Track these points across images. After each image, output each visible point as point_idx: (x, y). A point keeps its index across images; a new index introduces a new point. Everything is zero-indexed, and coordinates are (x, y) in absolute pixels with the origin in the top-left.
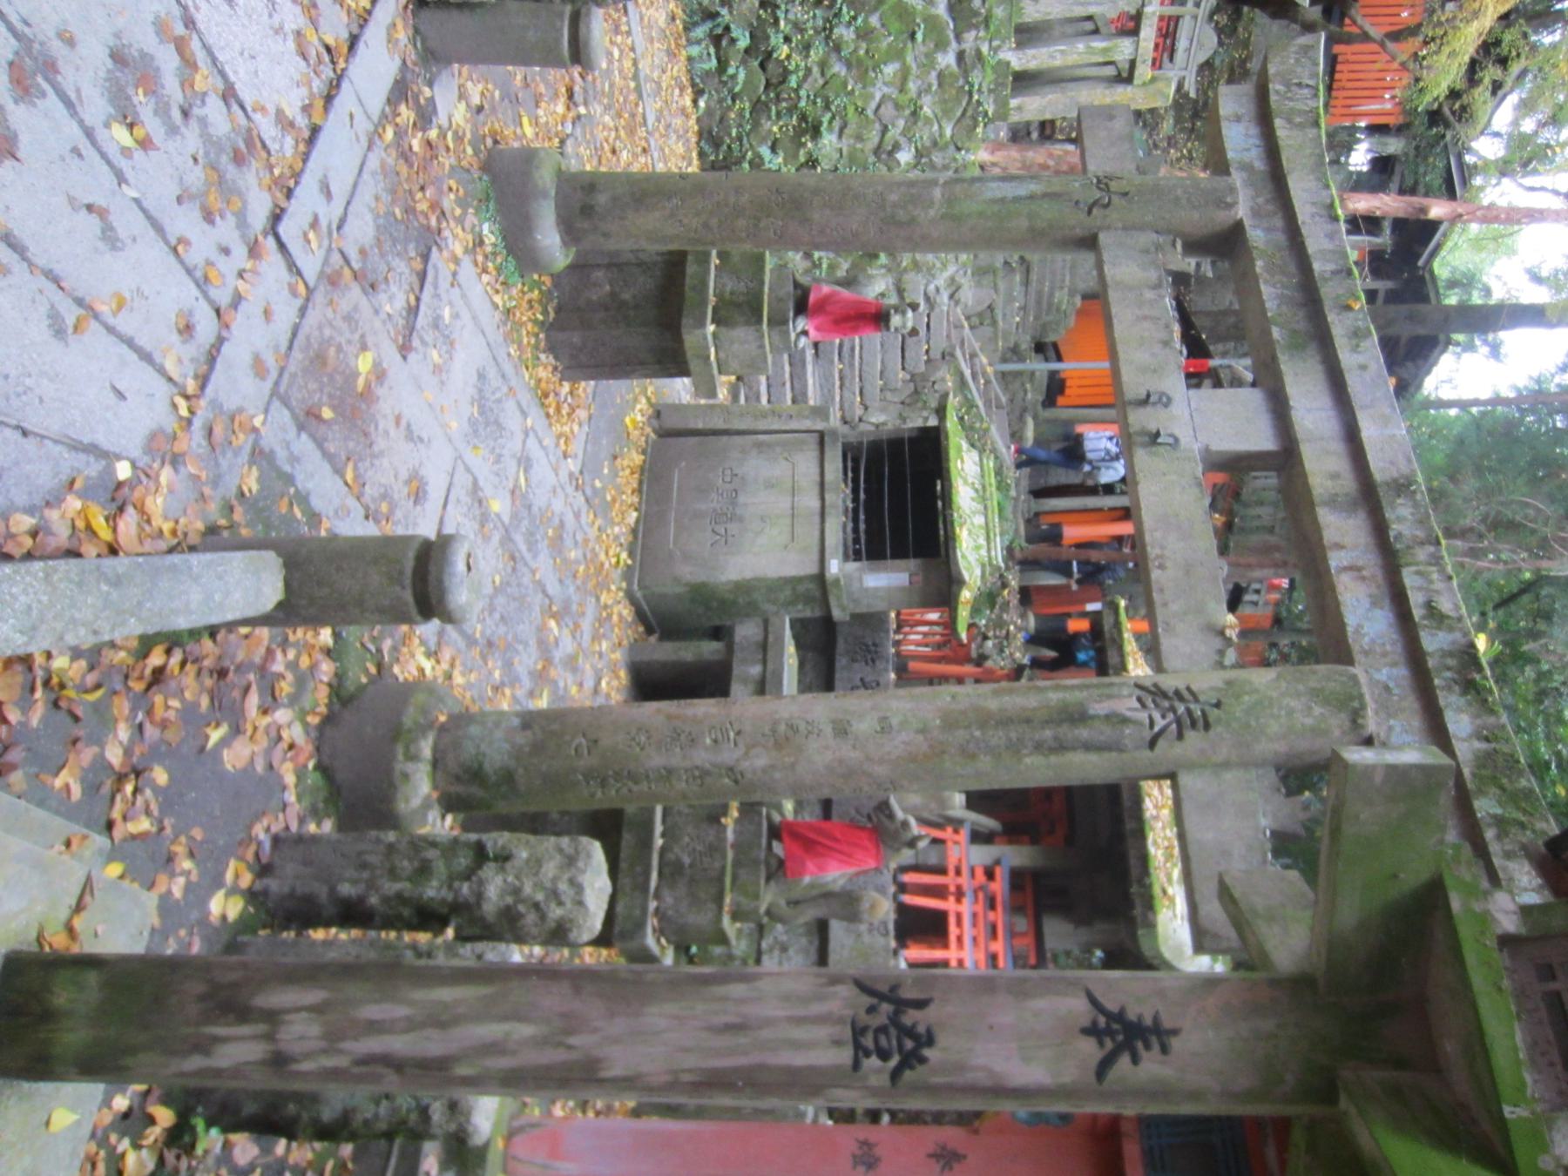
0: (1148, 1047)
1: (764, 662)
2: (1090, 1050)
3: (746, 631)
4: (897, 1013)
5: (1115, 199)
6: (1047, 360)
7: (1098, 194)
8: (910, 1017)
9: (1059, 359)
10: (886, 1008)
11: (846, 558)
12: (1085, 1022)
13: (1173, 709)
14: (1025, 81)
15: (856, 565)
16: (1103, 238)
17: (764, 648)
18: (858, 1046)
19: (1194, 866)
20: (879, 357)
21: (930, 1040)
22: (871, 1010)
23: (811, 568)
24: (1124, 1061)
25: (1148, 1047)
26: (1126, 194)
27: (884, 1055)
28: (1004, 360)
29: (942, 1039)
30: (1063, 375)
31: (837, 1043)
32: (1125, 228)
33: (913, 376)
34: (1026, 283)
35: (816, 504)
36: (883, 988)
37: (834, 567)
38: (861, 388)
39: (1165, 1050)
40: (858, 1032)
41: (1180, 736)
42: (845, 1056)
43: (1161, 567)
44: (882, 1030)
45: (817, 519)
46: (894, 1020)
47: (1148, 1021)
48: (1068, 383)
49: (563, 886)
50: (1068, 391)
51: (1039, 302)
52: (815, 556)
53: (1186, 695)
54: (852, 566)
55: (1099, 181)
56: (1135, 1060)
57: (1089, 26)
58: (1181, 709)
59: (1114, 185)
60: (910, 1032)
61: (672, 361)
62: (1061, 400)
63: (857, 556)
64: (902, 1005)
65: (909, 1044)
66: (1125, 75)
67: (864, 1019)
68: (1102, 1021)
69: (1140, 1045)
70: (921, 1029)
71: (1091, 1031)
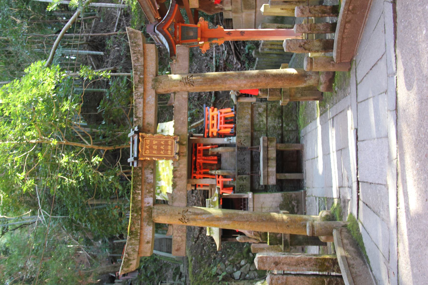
1: (268, 171)
3: (272, 181)
5: (181, 213)
7: (185, 214)
11: (247, 198)
13: (188, 81)
17: (267, 176)
23: (256, 195)
26: (179, 213)
41: (187, 77)
43: (185, 113)
49: (290, 42)
52: (255, 200)
55: (185, 219)
58: (187, 81)
63: (244, 199)
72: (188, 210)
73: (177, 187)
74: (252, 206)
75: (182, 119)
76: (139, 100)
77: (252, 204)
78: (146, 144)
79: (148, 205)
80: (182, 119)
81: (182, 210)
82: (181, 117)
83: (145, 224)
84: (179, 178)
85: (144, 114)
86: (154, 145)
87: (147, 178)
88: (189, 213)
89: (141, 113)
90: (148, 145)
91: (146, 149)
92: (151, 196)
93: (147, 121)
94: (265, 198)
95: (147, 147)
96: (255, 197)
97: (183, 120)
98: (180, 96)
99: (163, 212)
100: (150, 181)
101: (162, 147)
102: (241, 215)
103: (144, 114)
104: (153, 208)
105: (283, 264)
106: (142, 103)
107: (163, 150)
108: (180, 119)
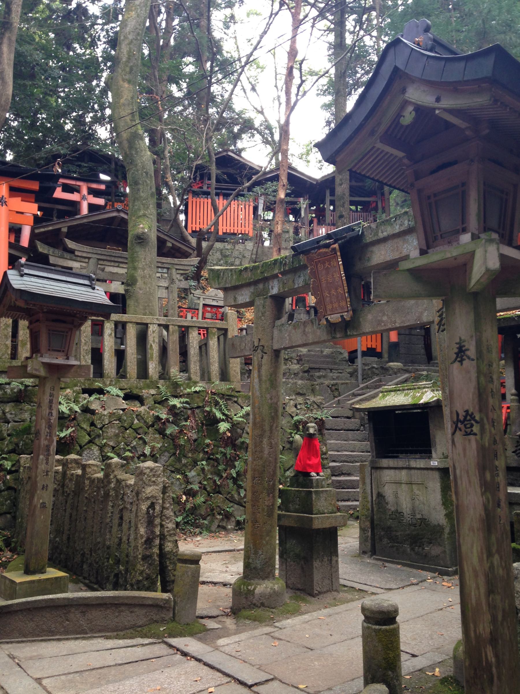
0: (464, 346)
2: (466, 363)
4: (461, 421)
6: (357, 358)
8: (461, 418)
9: (356, 351)
10: (459, 425)
12: (459, 364)
14: (224, 376)
15: (433, 452)
16: (275, 348)
18: (470, 434)
19: (512, 306)
20: (350, 442)
21: (467, 411)
22: (460, 430)
23: (436, 475)
24: (468, 353)
25: (464, 346)
26: (259, 340)
27: (472, 426)
28: (357, 380)
29: (466, 408)
30: (365, 349)
31: (469, 440)
32: (272, 340)
33: (362, 425)
34: (319, 369)
35: (404, 472)
36: (454, 426)
37: (434, 463)
38: (348, 448)
39: (464, 341)
40: (467, 434)
42: (472, 437)
43: (395, 322)
44: (465, 426)
45: (413, 471)
46: (462, 422)
47: (458, 346)
48: (369, 346)
50: (374, 347)
51: (328, 363)
53: (440, 312)
54: (434, 455)
55: (254, 350)
56: (467, 350)
57: (203, 348)
59: (256, 344)
60: (465, 417)
61: (330, 536)
62: (379, 350)
63: (430, 452)
64: (458, 420)
65: (468, 418)
66: (223, 332)
67: (463, 433)
68: (459, 359)
69: (464, 348)
70: (464, 414)
71: (461, 362)
72: (266, 353)
73: (293, 331)
74: (418, 466)
75: (385, 318)
76: (406, 222)
77: (422, 466)
78: (329, 261)
79: (270, 287)
80: (385, 318)
81: (266, 344)
82: (387, 315)
83: (252, 289)
84: (304, 331)
85: (385, 240)
86: (333, 276)
87: (299, 277)
88: (260, 356)
89: (385, 234)
90: (330, 264)
91: (324, 263)
92: (279, 290)
93: (375, 249)
94: (434, 491)
95: (327, 265)
96: (434, 472)
97: (383, 322)
98: (425, 306)
99: (260, 315)
100: (296, 282)
101: (333, 292)
102: (262, 442)
103: (385, 240)
104: (266, 298)
105: (137, 505)
106: (402, 229)
107: (329, 293)
108: (384, 314)
